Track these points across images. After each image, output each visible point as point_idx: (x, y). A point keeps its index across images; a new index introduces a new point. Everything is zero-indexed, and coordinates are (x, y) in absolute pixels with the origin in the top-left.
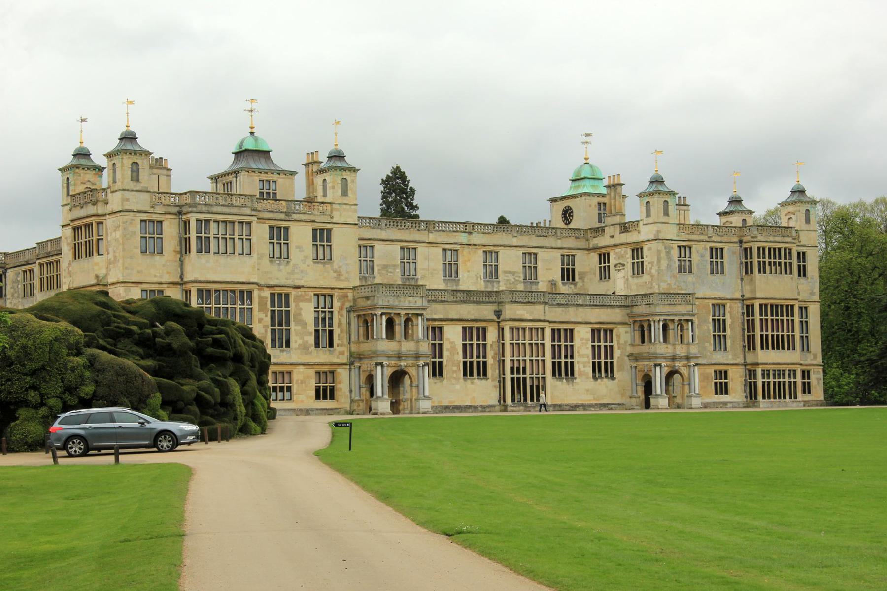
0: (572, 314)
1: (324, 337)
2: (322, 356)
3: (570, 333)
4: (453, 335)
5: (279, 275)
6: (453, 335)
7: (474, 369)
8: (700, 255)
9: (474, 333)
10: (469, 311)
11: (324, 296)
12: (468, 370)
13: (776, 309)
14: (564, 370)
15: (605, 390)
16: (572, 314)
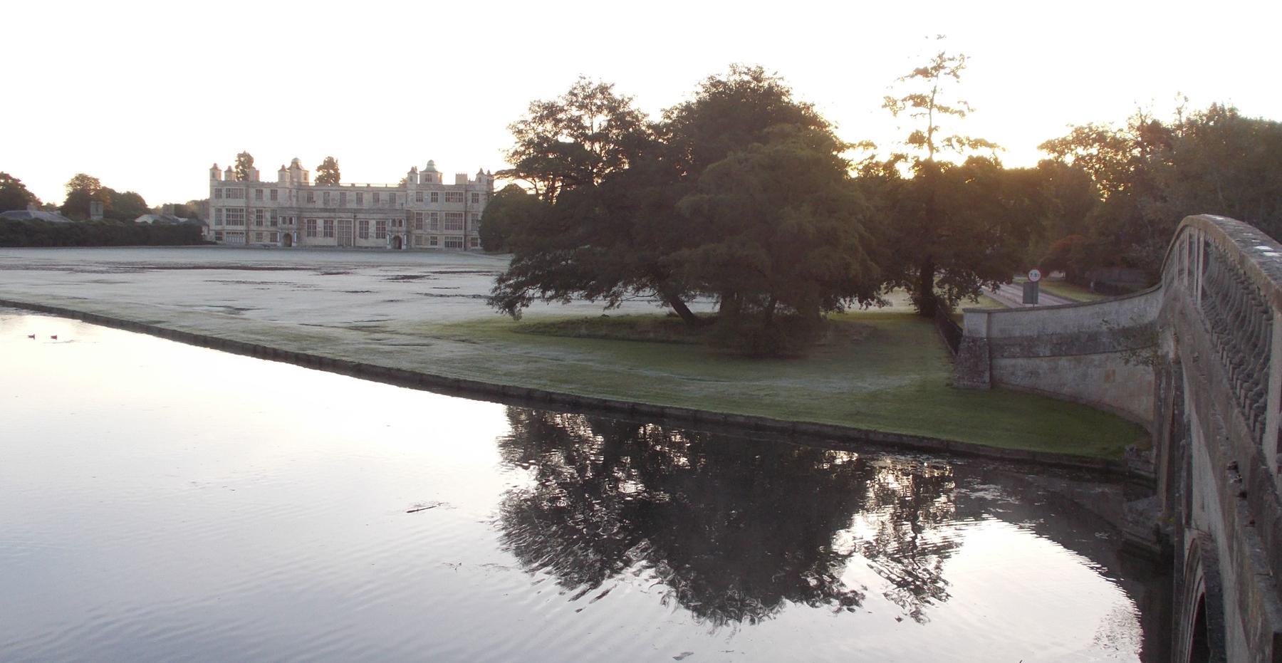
0: (367, 216)
1: (274, 223)
2: (273, 229)
3: (367, 223)
4: (320, 223)
5: (259, 204)
6: (320, 223)
7: (329, 233)
8: (427, 196)
9: (328, 224)
10: (327, 214)
11: (274, 211)
12: (326, 235)
13: (454, 215)
14: (365, 235)
15: (381, 242)
16: (367, 216)
